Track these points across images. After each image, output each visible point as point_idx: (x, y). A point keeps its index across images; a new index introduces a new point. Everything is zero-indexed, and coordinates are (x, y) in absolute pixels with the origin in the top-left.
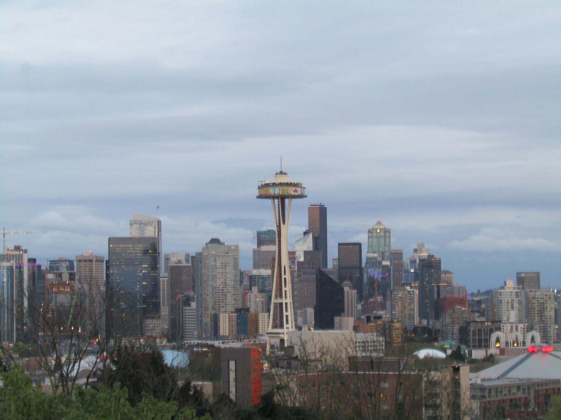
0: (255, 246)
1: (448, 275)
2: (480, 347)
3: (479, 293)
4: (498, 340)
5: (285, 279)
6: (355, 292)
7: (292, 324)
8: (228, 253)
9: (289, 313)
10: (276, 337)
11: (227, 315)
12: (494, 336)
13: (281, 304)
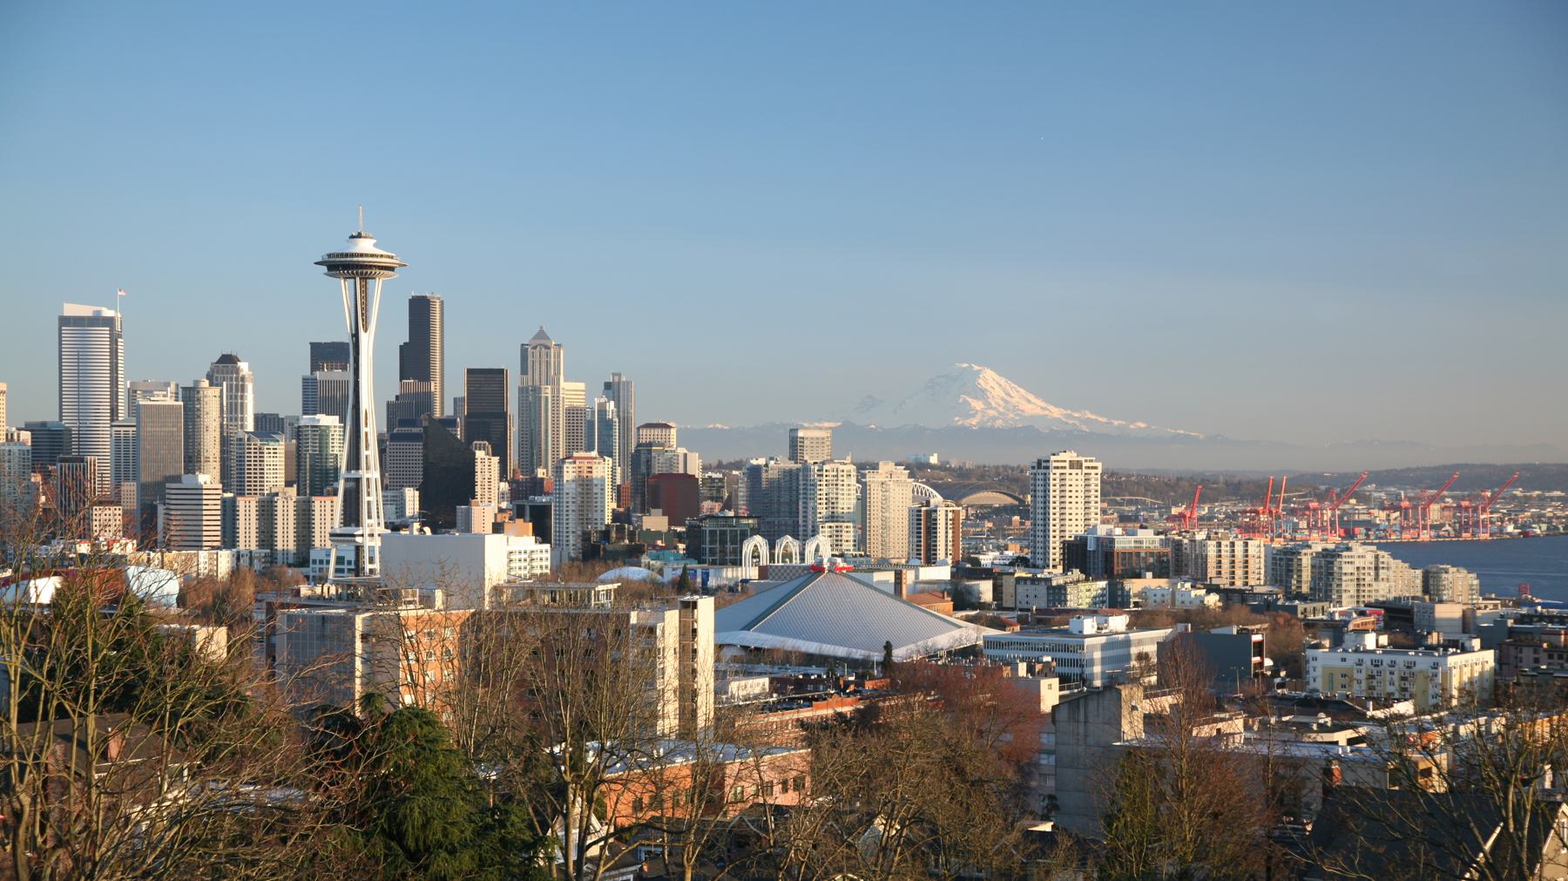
0: (308, 373)
2: (723, 563)
3: (720, 467)
4: (756, 555)
6: (496, 459)
9: (372, 498)
13: (358, 481)
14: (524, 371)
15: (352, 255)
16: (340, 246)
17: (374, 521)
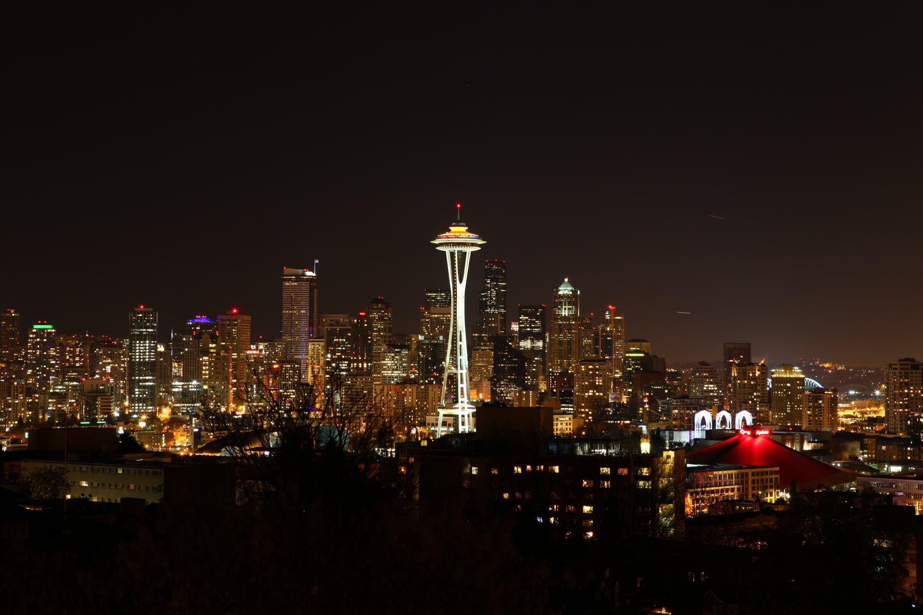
1: (644, 344)
2: (682, 428)
4: (703, 422)
9: (463, 386)
12: (698, 417)
13: (456, 374)
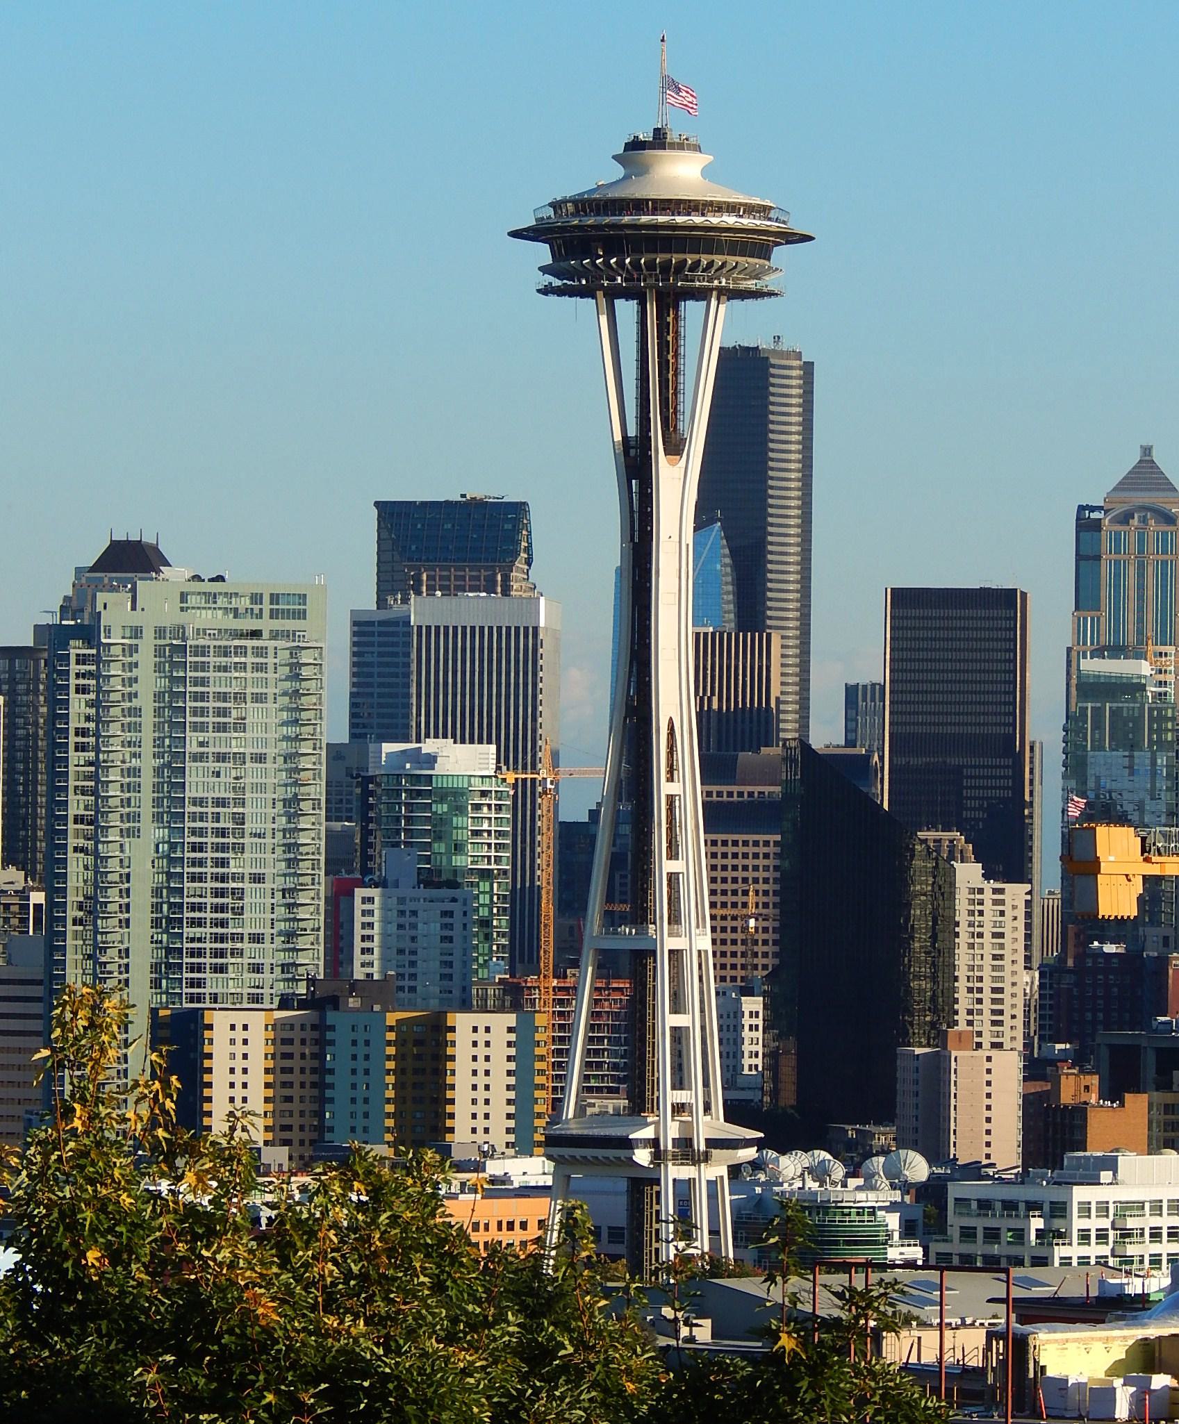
0: (367, 601)
5: (671, 799)
7: (706, 1084)
8: (256, 634)
10: (607, 1162)
11: (257, 1021)
14: (1085, 596)
15: (639, 205)
16: (595, 172)
17: (691, 1096)
